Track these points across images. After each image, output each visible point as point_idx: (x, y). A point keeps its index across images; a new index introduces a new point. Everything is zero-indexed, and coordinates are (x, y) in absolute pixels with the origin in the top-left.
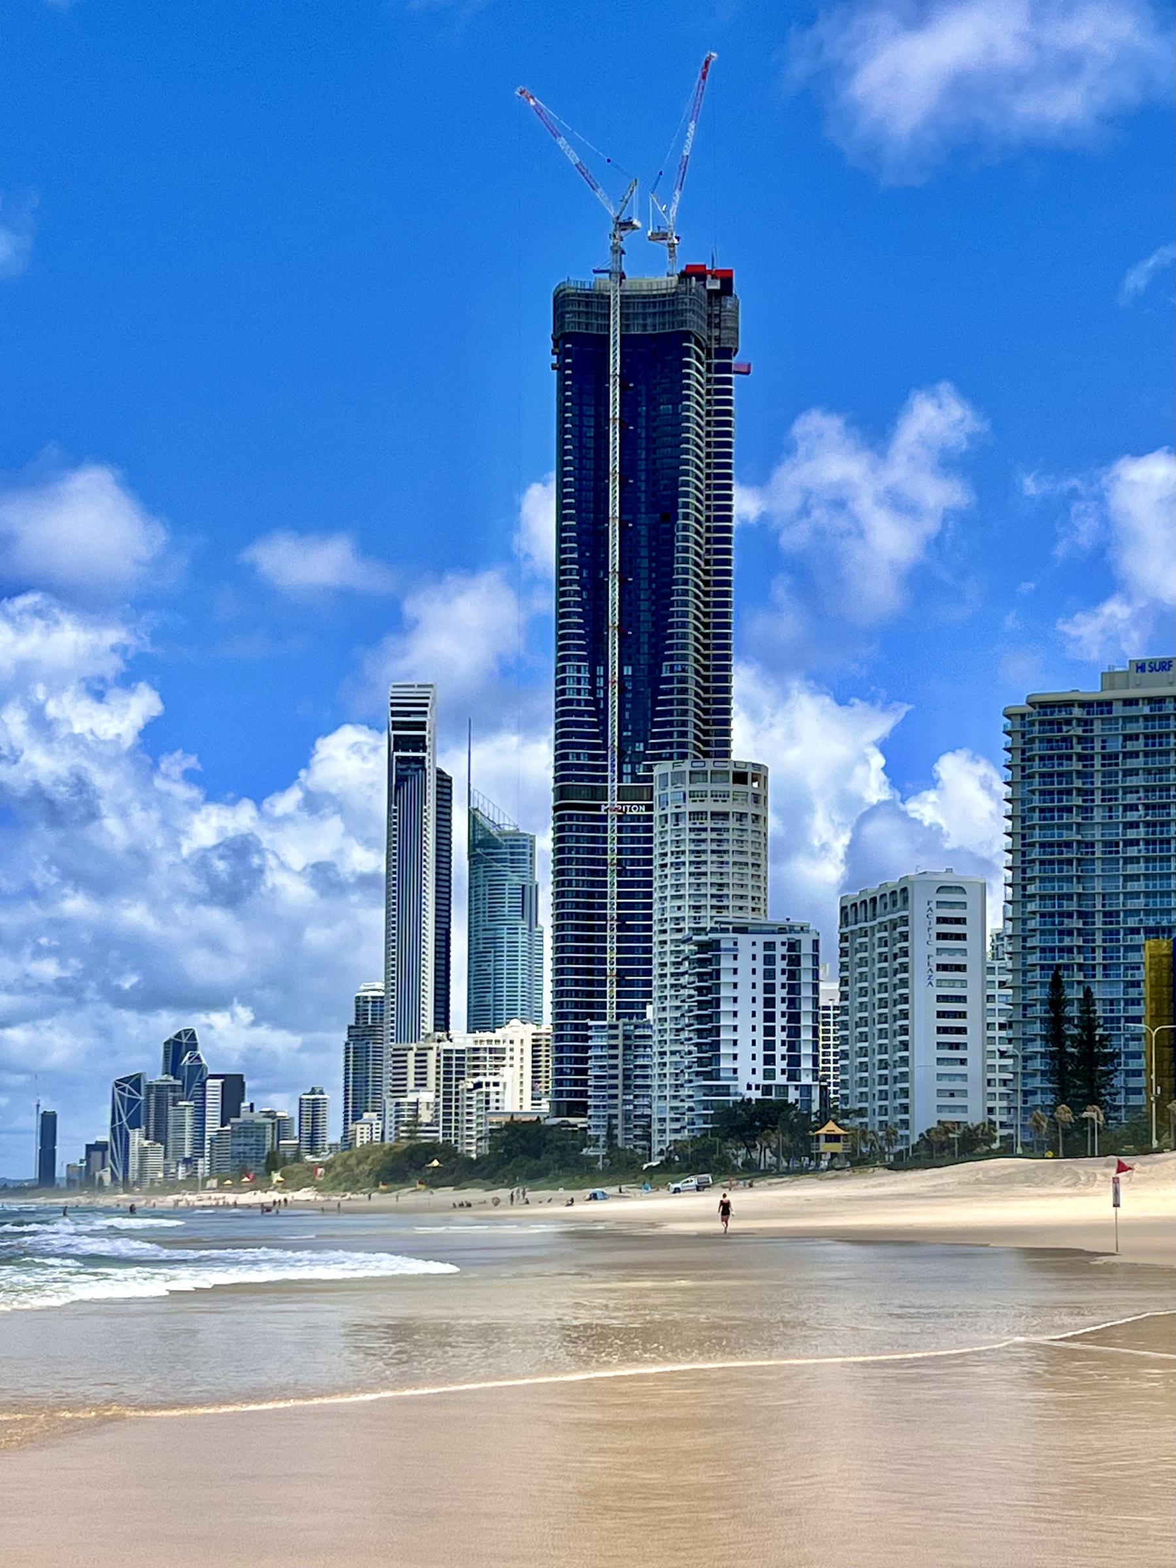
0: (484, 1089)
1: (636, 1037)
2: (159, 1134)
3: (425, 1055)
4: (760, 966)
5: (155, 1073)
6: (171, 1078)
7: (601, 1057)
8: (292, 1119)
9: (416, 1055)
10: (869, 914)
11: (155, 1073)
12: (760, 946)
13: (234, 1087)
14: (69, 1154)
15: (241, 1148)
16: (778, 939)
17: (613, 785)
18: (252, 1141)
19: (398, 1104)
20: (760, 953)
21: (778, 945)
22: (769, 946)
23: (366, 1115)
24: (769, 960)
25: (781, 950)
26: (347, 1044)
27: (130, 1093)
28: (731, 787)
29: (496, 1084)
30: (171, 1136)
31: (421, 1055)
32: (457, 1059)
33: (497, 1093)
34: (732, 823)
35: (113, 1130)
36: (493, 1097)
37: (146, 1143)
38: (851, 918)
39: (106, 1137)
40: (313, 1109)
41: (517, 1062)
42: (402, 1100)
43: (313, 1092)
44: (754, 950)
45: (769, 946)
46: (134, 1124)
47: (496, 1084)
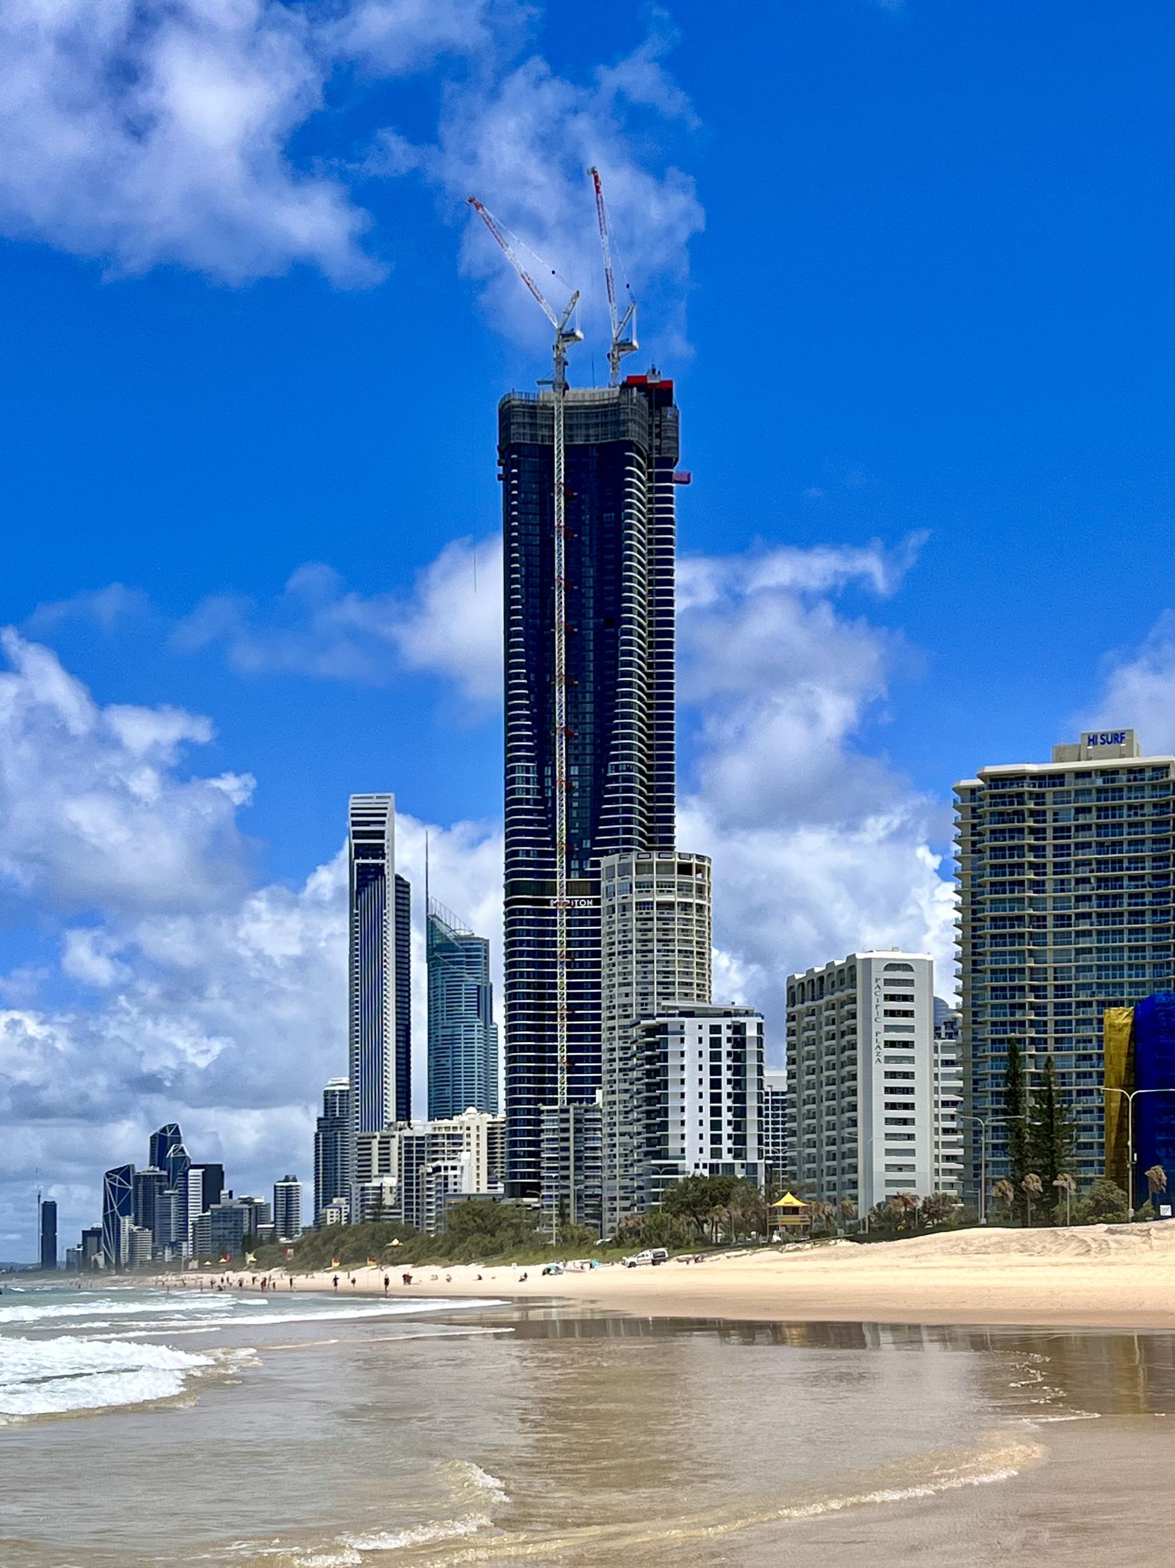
0: (442, 1173)
1: (587, 1120)
2: (146, 1220)
3: (388, 1143)
4: (706, 1049)
5: (143, 1166)
6: (157, 1169)
7: (553, 1139)
8: (268, 1205)
9: (380, 1143)
10: (816, 993)
11: (143, 1166)
12: (707, 1029)
13: (214, 1176)
14: (68, 1238)
15: (221, 1232)
16: (724, 1022)
17: (561, 880)
18: (231, 1225)
19: (363, 1189)
20: (707, 1036)
21: (724, 1028)
22: (715, 1029)
23: (335, 1200)
24: (715, 1043)
25: (726, 1034)
26: (317, 1135)
27: (120, 1183)
28: (677, 878)
29: (454, 1168)
30: (157, 1221)
31: (385, 1142)
32: (418, 1145)
33: (455, 1176)
34: (677, 914)
35: (106, 1217)
36: (451, 1180)
37: (135, 1228)
38: (798, 997)
39: (99, 1224)
40: (287, 1196)
41: (473, 1147)
42: (367, 1185)
43: (287, 1180)
44: (700, 1033)
45: (715, 1029)
46: (125, 1211)
47: (454, 1168)
